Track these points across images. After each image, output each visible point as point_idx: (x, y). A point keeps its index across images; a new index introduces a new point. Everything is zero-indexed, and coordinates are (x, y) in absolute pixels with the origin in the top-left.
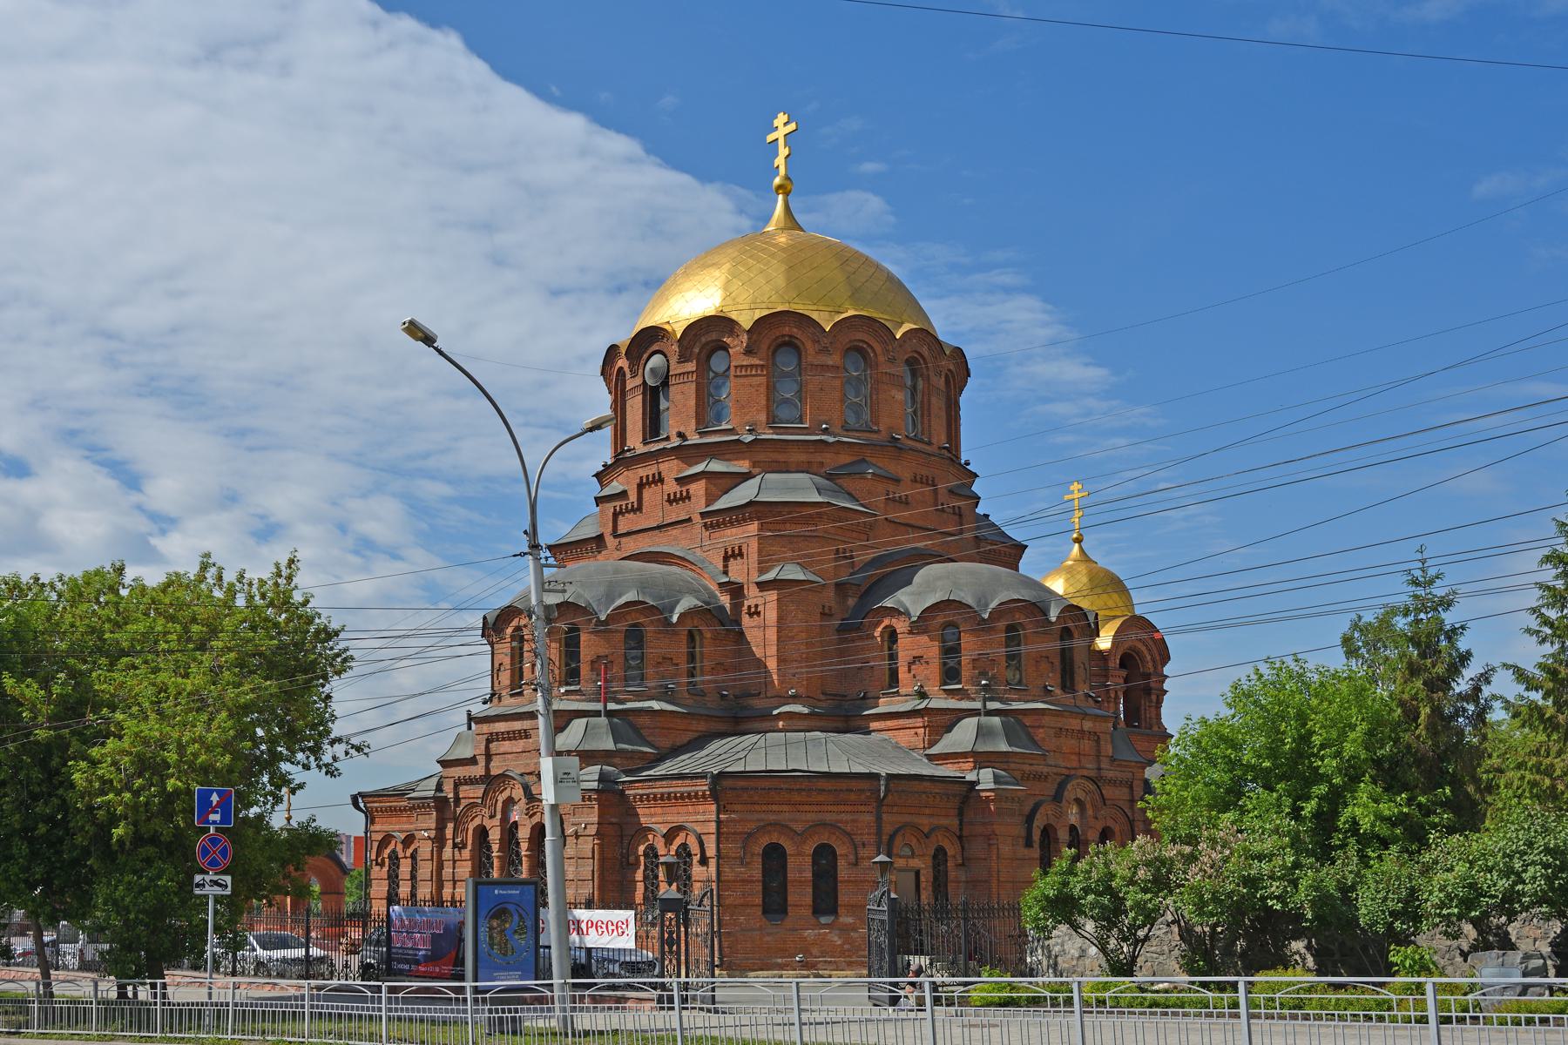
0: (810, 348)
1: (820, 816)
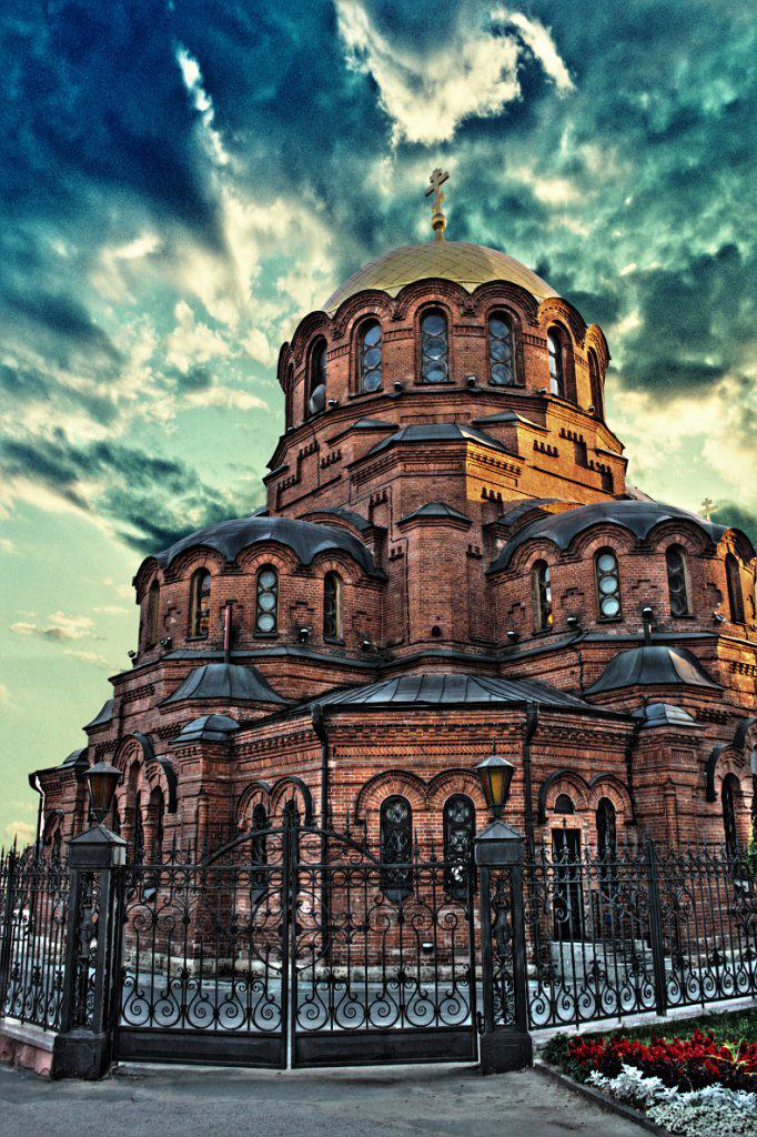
1: (453, 759)
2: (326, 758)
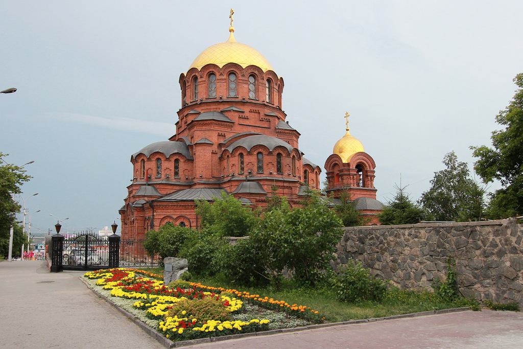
0: (218, 74)
2: (153, 212)
